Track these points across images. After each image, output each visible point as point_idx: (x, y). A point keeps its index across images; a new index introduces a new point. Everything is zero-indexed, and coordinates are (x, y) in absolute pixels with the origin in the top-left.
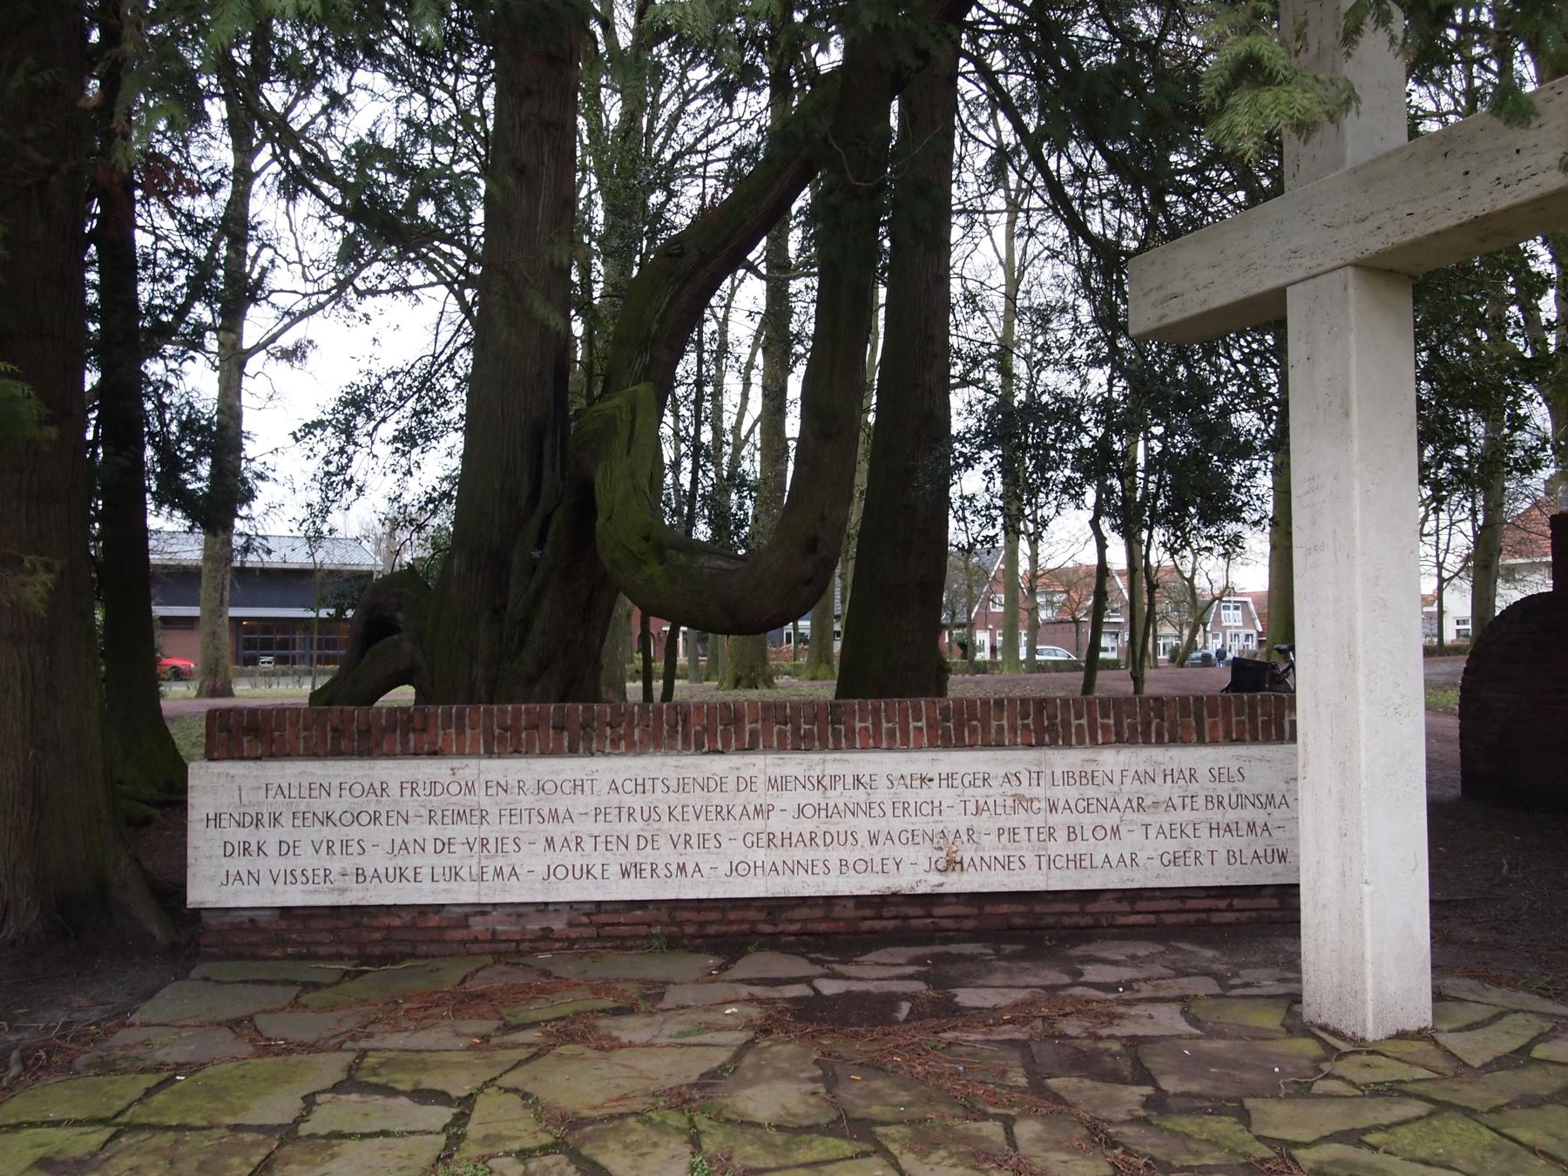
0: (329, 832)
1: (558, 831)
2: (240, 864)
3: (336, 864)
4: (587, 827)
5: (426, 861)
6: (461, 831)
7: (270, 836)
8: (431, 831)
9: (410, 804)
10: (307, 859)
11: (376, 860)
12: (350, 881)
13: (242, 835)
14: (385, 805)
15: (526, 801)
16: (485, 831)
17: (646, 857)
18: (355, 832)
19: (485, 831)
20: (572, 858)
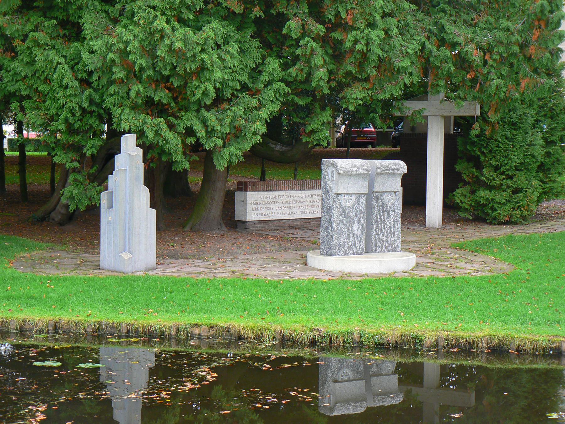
0: (268, 206)
1: (300, 205)
2: (255, 212)
3: (269, 212)
4: (305, 204)
5: (282, 211)
6: (287, 205)
7: (259, 206)
8: (282, 205)
9: (280, 200)
10: (264, 211)
11: (275, 211)
12: (270, 215)
13: (255, 206)
14: (276, 200)
15: (296, 199)
16: (291, 205)
17: (313, 209)
18: (272, 206)
19: (291, 205)
20: (303, 210)
